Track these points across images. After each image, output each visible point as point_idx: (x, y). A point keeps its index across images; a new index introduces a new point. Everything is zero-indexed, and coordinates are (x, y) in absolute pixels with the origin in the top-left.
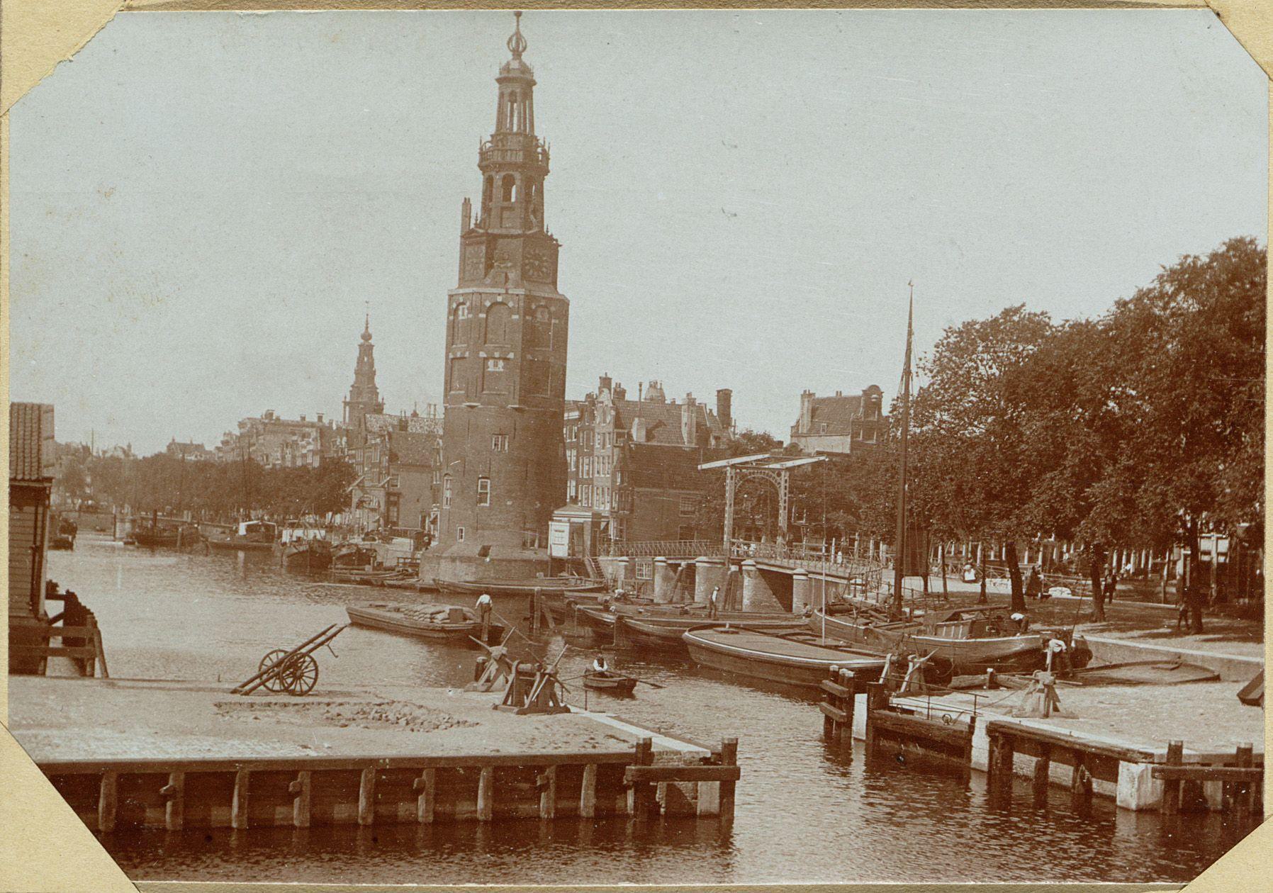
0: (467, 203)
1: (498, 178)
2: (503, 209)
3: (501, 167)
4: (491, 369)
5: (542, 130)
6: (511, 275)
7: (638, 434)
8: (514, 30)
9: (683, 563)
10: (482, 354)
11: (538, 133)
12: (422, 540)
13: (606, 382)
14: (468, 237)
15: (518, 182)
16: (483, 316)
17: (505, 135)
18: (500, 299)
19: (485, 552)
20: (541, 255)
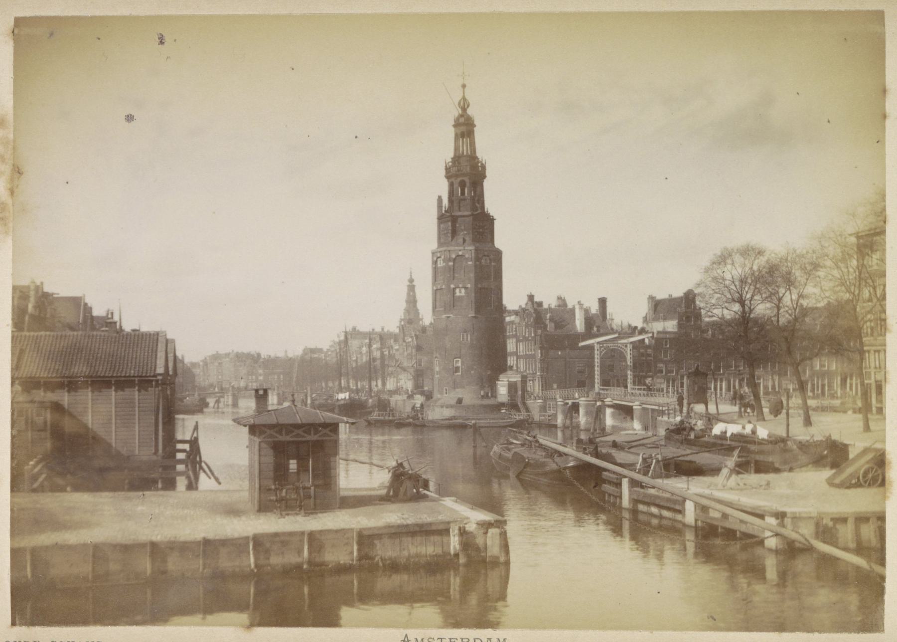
0: (440, 199)
1: (456, 182)
2: (460, 201)
3: (457, 176)
4: (458, 293)
5: (483, 152)
6: (467, 238)
7: (550, 327)
9: (570, 402)
10: (452, 286)
11: (479, 154)
12: (429, 396)
13: (531, 298)
14: (441, 218)
15: (468, 184)
16: (451, 264)
17: (459, 157)
18: (460, 253)
19: (460, 401)
20: (482, 226)
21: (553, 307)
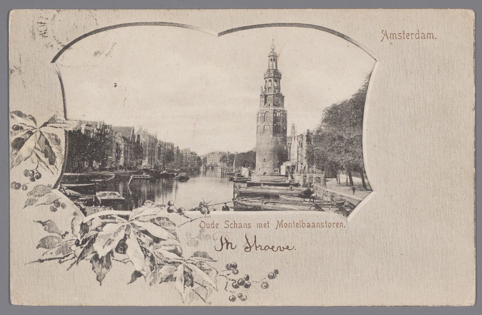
1: (268, 80)
4: (266, 128)
10: (264, 125)
14: (261, 95)
19: (265, 173)
20: (279, 99)
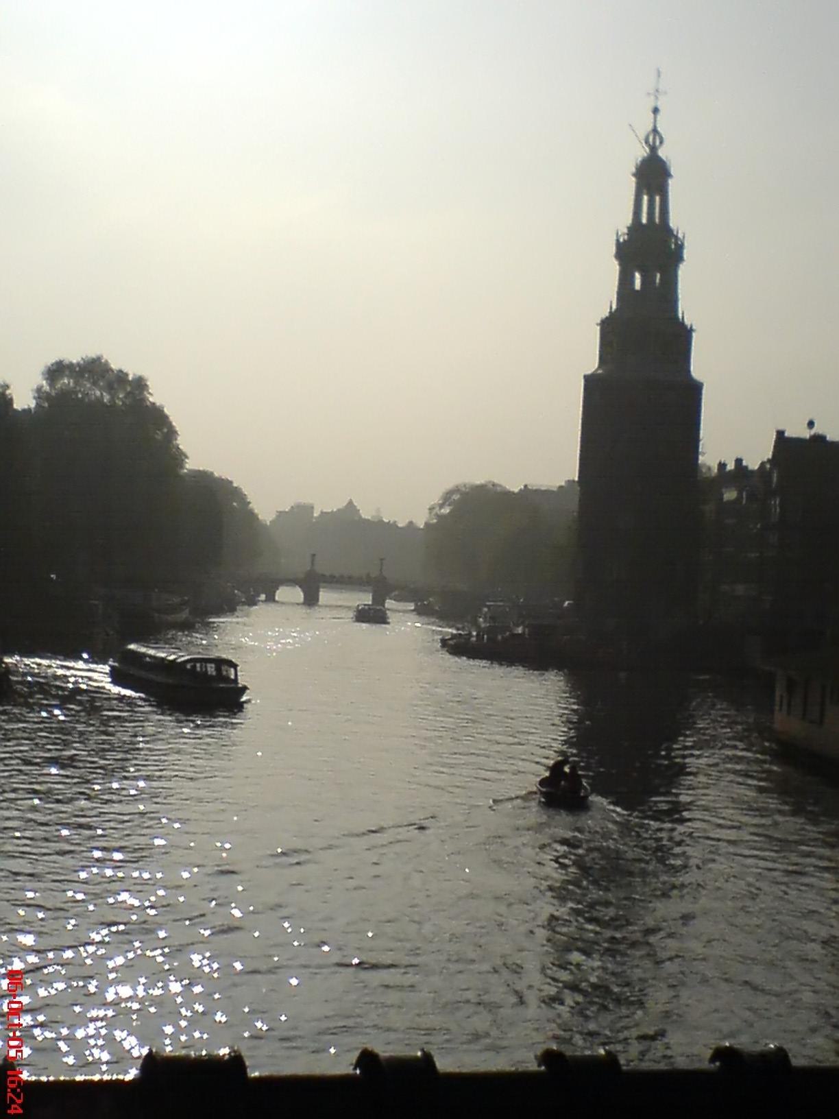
8: (650, 127)
21: (753, 464)
